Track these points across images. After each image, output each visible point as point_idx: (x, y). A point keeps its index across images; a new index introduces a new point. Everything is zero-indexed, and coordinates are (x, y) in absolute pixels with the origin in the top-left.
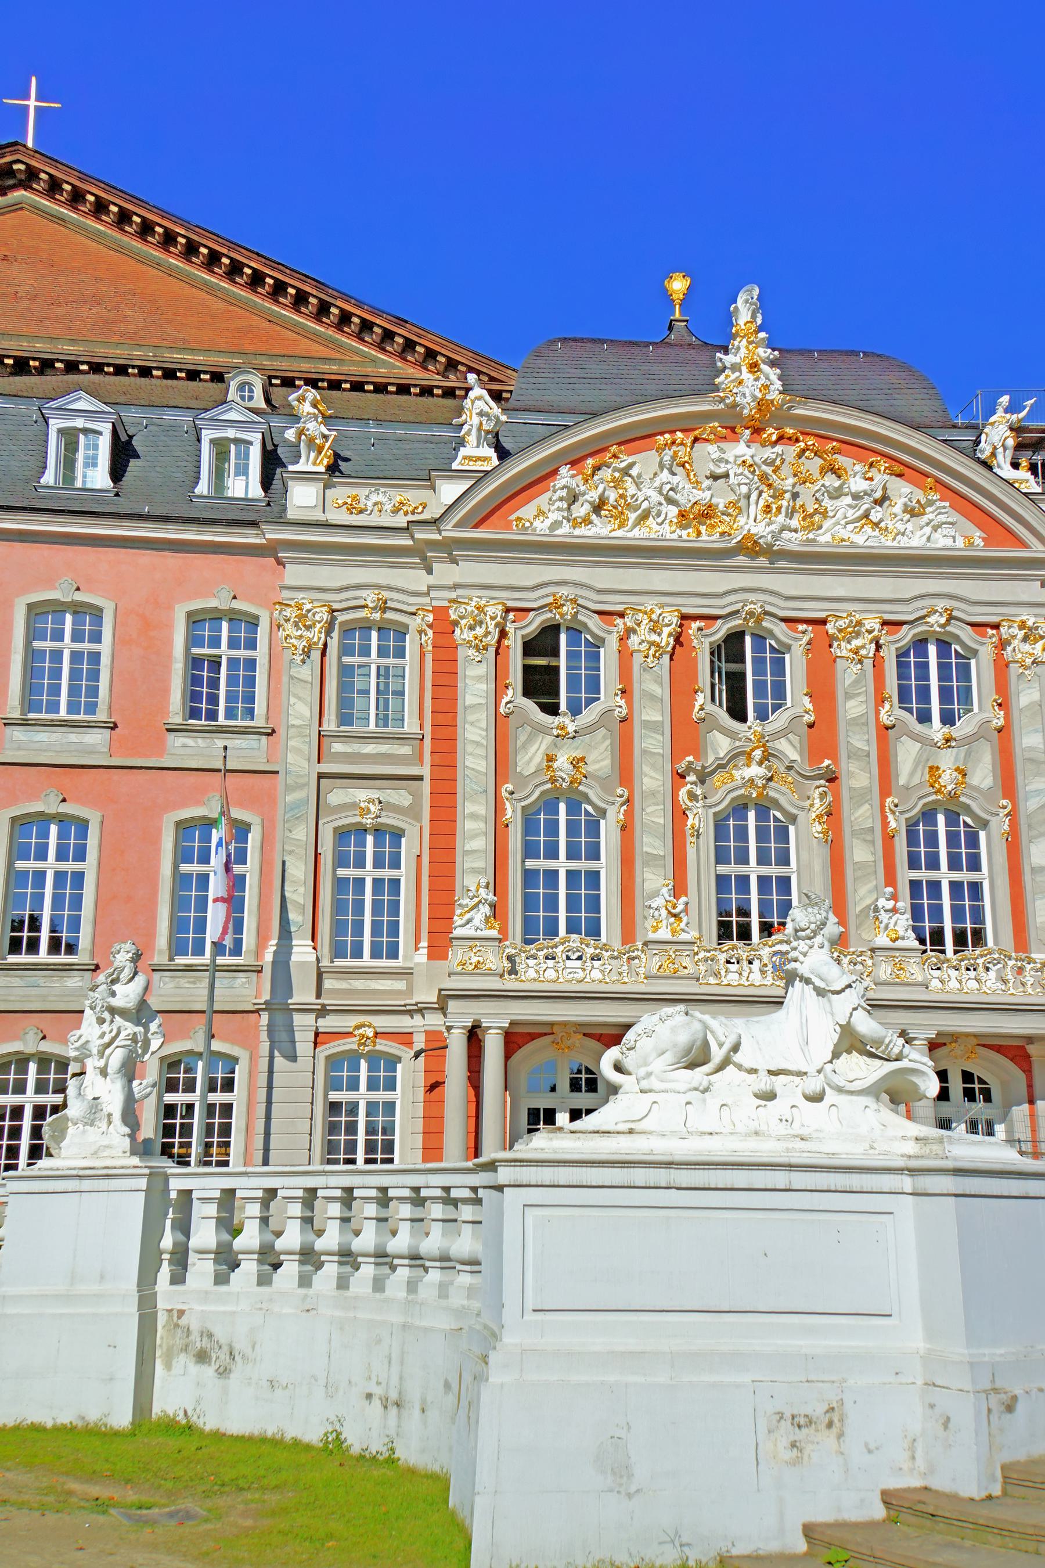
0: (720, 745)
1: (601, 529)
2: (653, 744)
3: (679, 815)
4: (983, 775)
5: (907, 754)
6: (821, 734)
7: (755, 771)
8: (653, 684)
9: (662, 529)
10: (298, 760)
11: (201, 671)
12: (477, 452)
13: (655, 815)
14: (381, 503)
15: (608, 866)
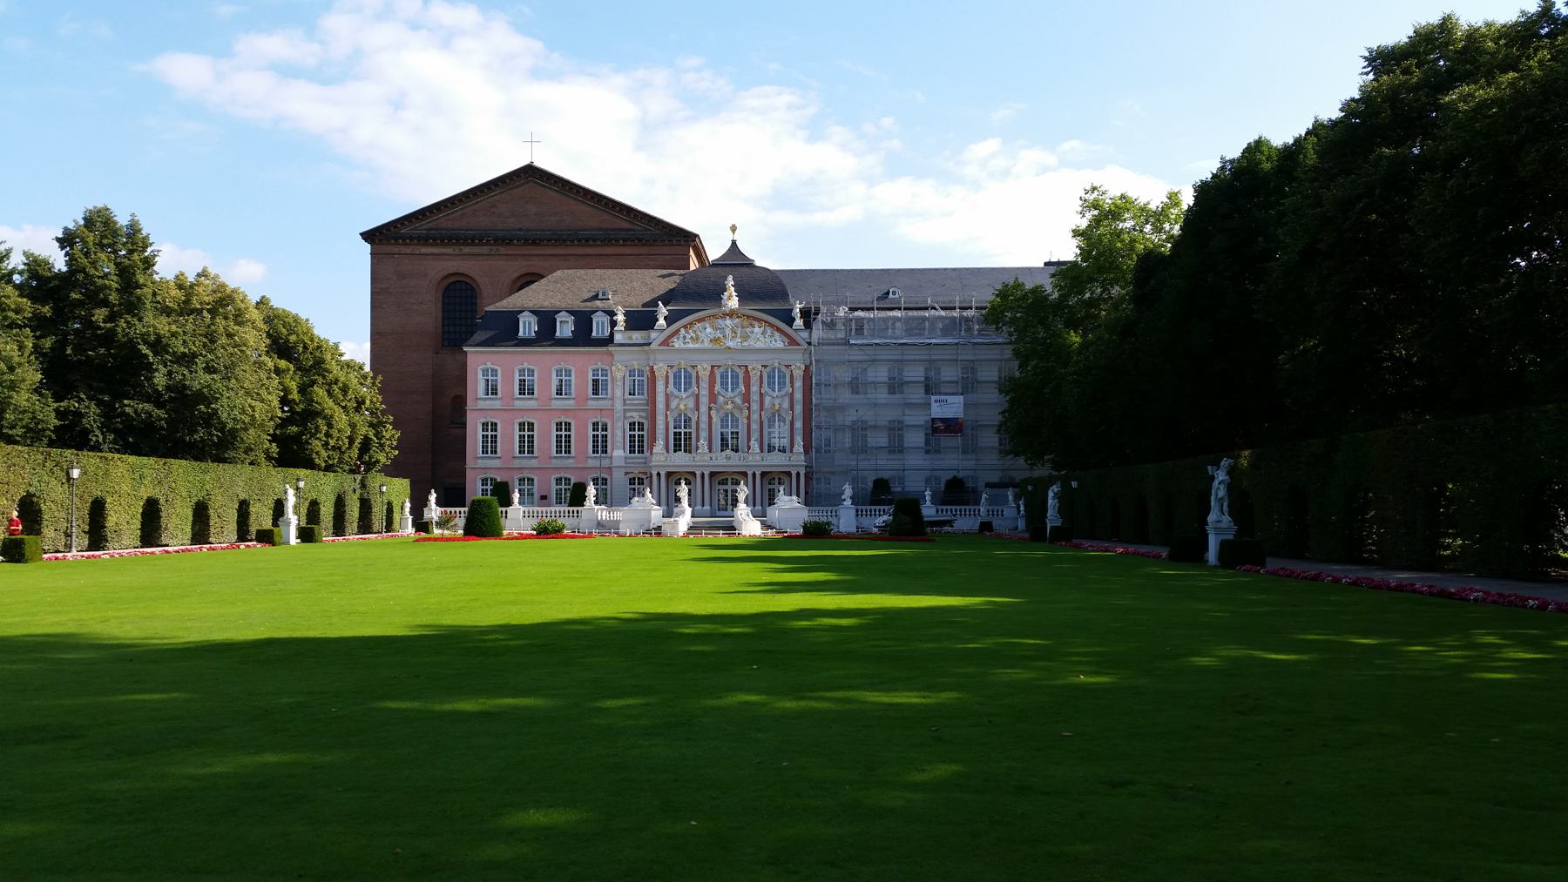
0: (721, 399)
1: (691, 346)
2: (704, 400)
3: (710, 418)
4: (786, 405)
5: (767, 400)
6: (746, 398)
7: (730, 406)
8: (705, 385)
9: (707, 345)
10: (619, 406)
11: (596, 382)
12: (662, 322)
13: (704, 418)
14: (637, 336)
15: (693, 431)
